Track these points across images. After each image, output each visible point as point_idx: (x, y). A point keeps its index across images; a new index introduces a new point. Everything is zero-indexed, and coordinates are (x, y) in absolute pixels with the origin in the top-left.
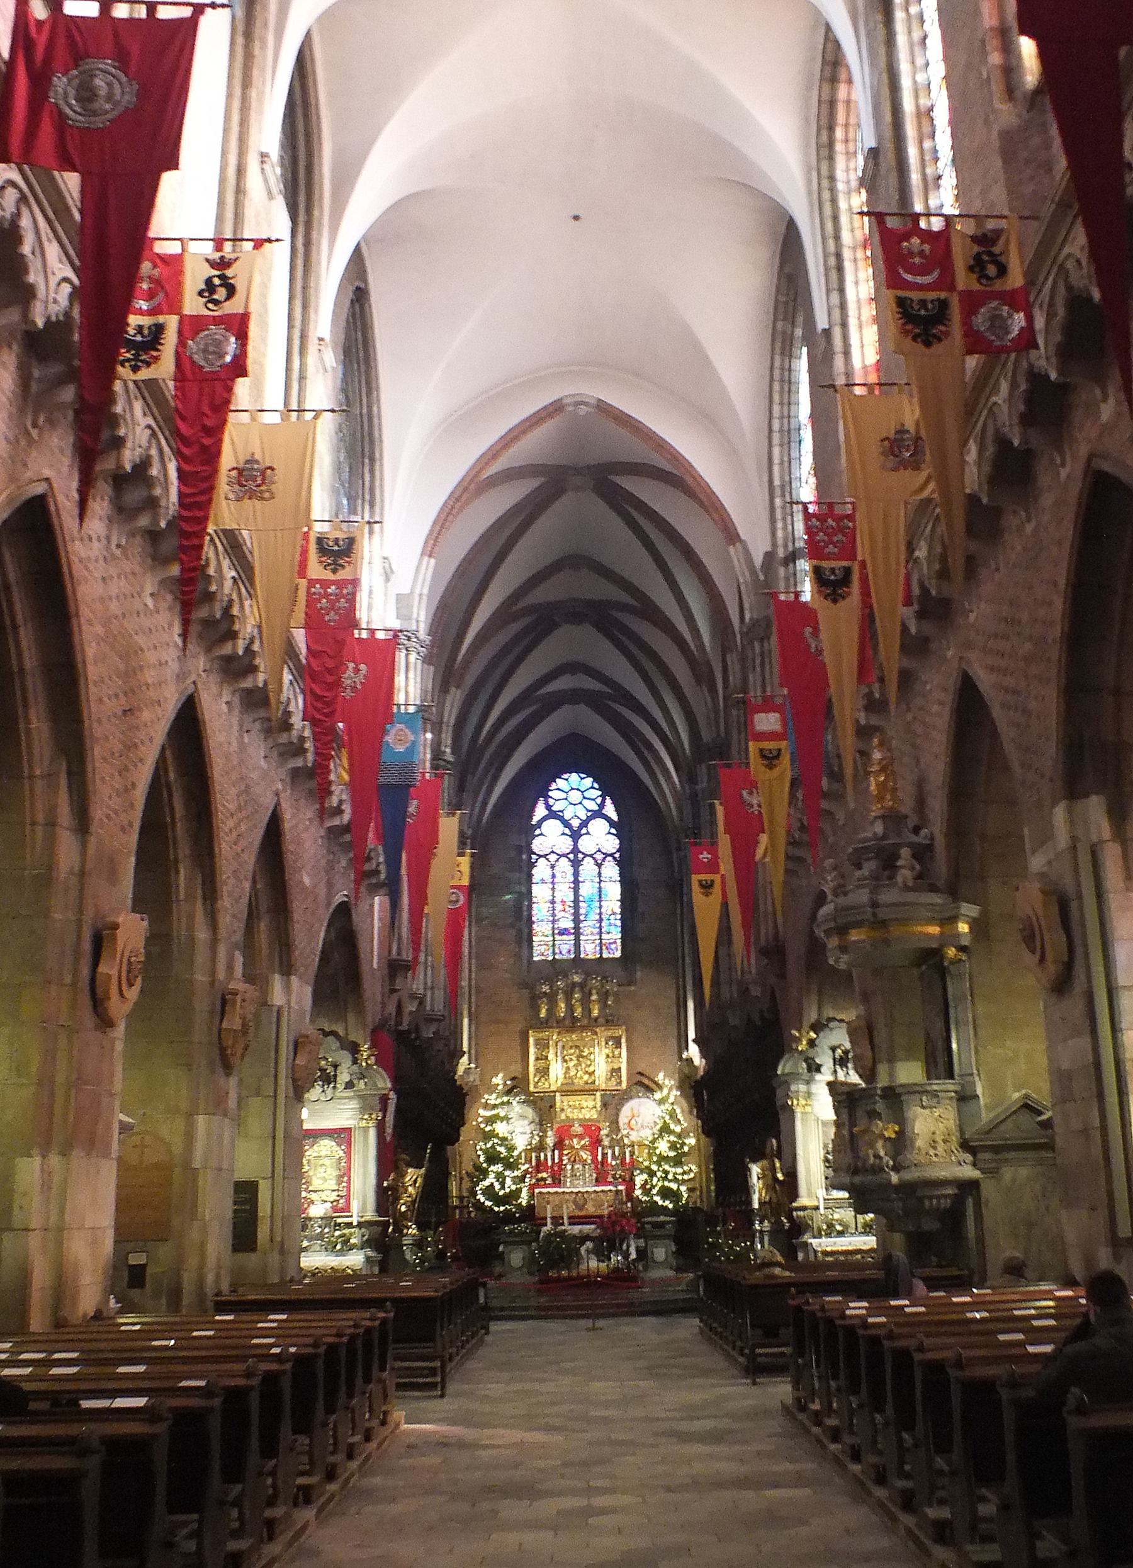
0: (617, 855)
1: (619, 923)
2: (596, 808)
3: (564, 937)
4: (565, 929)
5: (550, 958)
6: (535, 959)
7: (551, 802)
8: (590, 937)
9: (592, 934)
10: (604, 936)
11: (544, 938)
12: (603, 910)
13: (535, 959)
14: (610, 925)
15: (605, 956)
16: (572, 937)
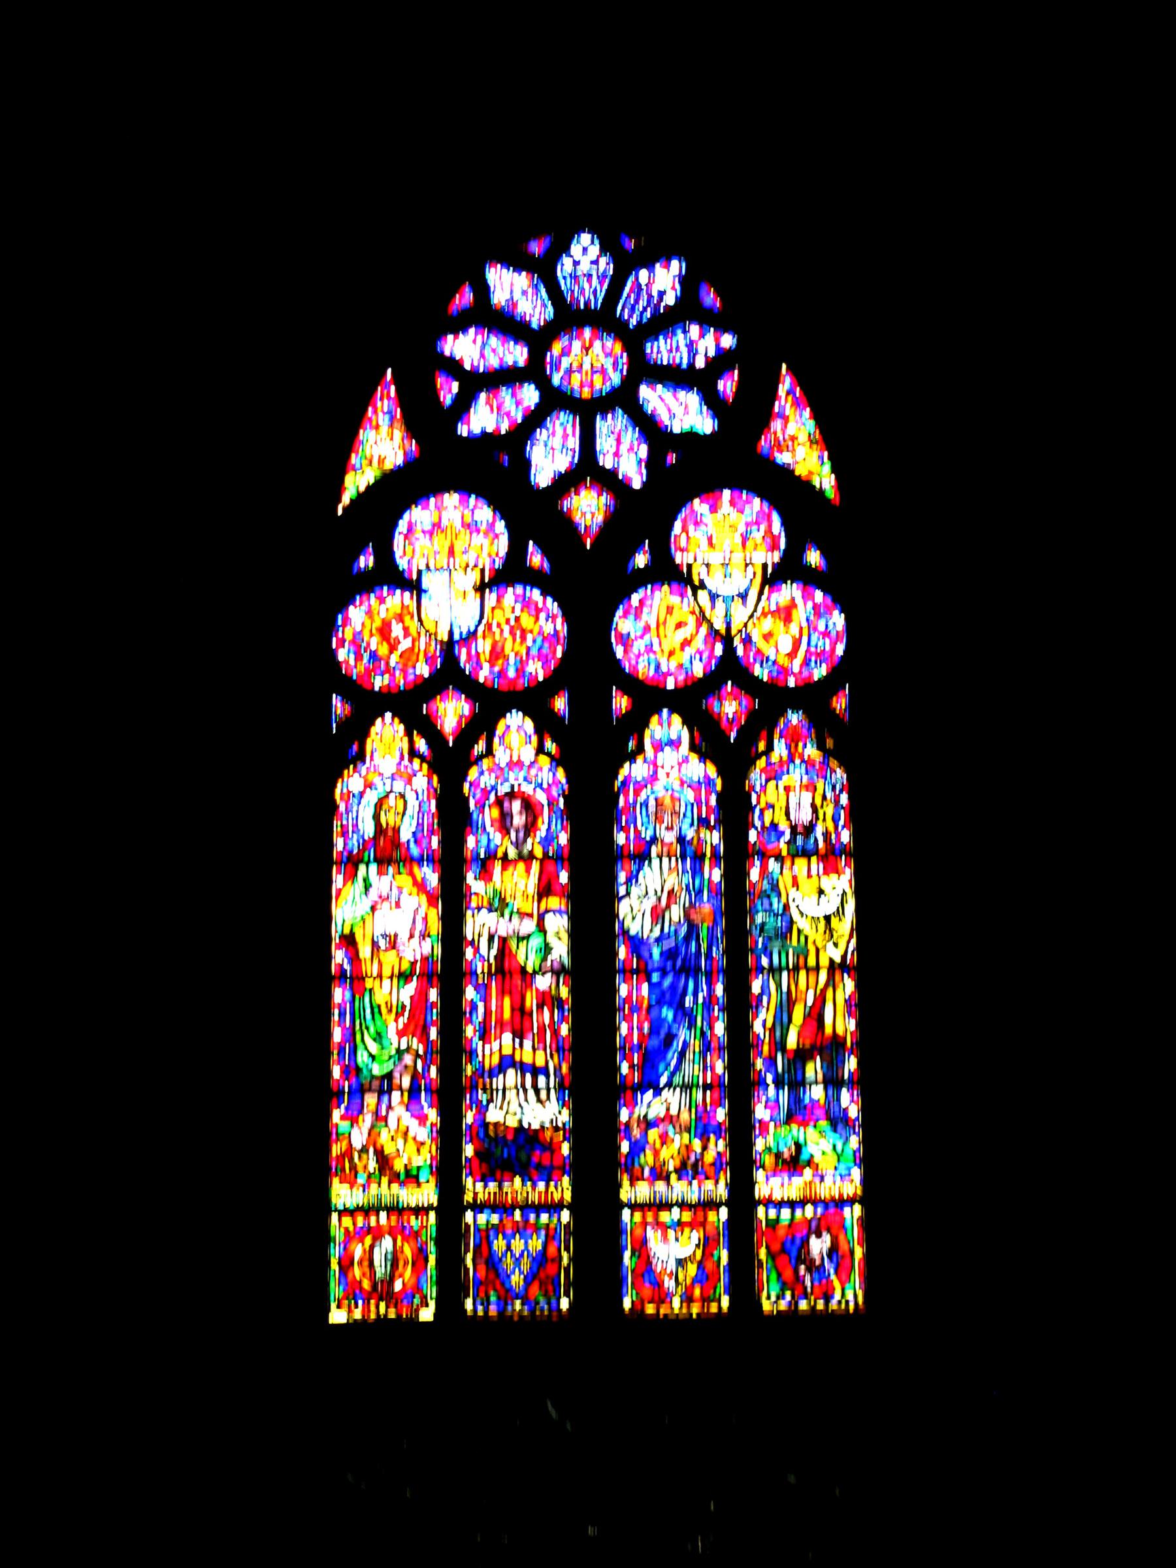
0: (840, 703)
1: (850, 1103)
2: (705, 424)
3: (516, 1187)
4: (527, 1138)
5: (427, 1315)
6: (337, 1316)
7: (447, 392)
8: (680, 1189)
9: (689, 1168)
10: (767, 1185)
11: (385, 1191)
12: (761, 1023)
13: (337, 1316)
14: (798, 1113)
15: (773, 1299)
16: (564, 1189)
